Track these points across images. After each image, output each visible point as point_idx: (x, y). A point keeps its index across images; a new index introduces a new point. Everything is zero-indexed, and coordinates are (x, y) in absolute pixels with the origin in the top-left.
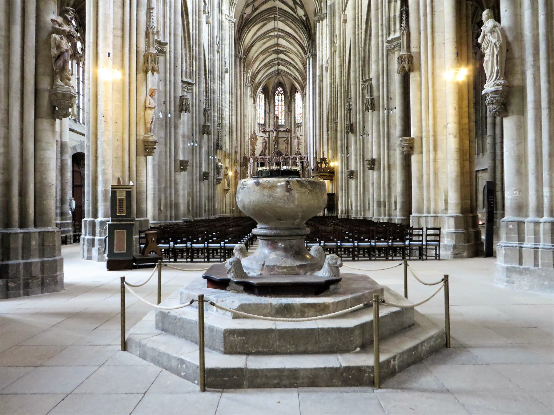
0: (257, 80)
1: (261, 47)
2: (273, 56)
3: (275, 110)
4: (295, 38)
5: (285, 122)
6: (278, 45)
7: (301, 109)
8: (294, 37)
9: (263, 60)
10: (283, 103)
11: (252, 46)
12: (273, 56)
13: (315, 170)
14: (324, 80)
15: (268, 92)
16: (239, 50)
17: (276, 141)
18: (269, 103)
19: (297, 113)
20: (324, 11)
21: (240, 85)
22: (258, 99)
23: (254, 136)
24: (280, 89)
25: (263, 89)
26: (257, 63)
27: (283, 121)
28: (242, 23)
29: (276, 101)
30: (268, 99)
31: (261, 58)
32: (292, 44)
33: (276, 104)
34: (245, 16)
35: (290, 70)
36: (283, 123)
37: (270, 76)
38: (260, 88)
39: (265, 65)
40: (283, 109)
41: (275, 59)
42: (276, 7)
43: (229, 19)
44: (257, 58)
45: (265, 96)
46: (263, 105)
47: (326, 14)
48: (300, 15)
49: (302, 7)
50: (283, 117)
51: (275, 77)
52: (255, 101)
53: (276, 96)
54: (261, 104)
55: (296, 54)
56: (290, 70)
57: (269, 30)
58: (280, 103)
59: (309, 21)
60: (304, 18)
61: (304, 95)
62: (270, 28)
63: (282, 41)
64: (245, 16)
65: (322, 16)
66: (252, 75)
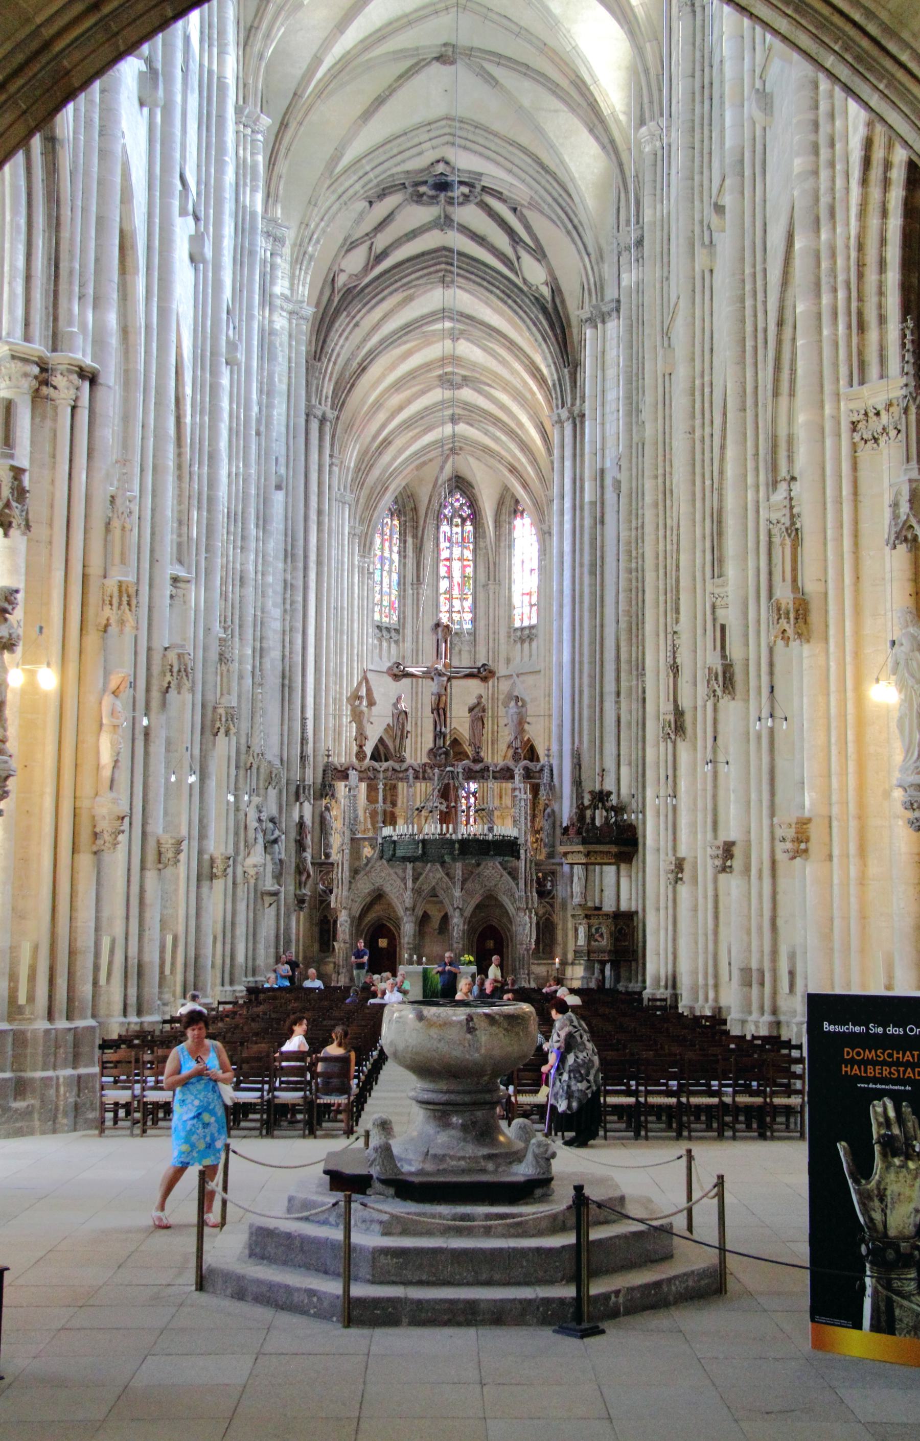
0: (376, 472)
1: (393, 367)
2: (437, 395)
3: (437, 577)
4: (512, 346)
5: (474, 621)
6: (455, 359)
7: (536, 574)
8: (512, 342)
9: (401, 408)
10: (468, 554)
11: (363, 369)
12: (437, 395)
13: (572, 831)
14: (610, 518)
15: (415, 509)
16: (319, 391)
17: (440, 710)
18: (419, 550)
19: (518, 589)
20: (611, 293)
21: (320, 512)
22: (378, 540)
23: (363, 692)
24: (458, 500)
25: (396, 502)
26: (381, 416)
27: (468, 616)
28: (330, 300)
29: (444, 544)
30: (415, 536)
31: (395, 400)
32: (503, 362)
33: (445, 554)
34: (341, 280)
35: (496, 439)
36: (468, 626)
37: (421, 460)
38: (387, 500)
39: (407, 425)
40: (469, 571)
41: (443, 402)
42: (451, 250)
43: (290, 307)
44: (378, 405)
45: (403, 526)
46: (396, 557)
47: (618, 301)
48: (531, 279)
49: (539, 253)
50: (468, 604)
51: (440, 459)
52: (366, 547)
53: (445, 528)
54: (387, 554)
55: (519, 397)
56: (496, 439)
57: (423, 317)
58: (457, 551)
59: (563, 302)
60: (546, 291)
61: (544, 535)
62: (425, 311)
63: (467, 349)
64: (341, 280)
65: (605, 309)
66: (360, 460)
